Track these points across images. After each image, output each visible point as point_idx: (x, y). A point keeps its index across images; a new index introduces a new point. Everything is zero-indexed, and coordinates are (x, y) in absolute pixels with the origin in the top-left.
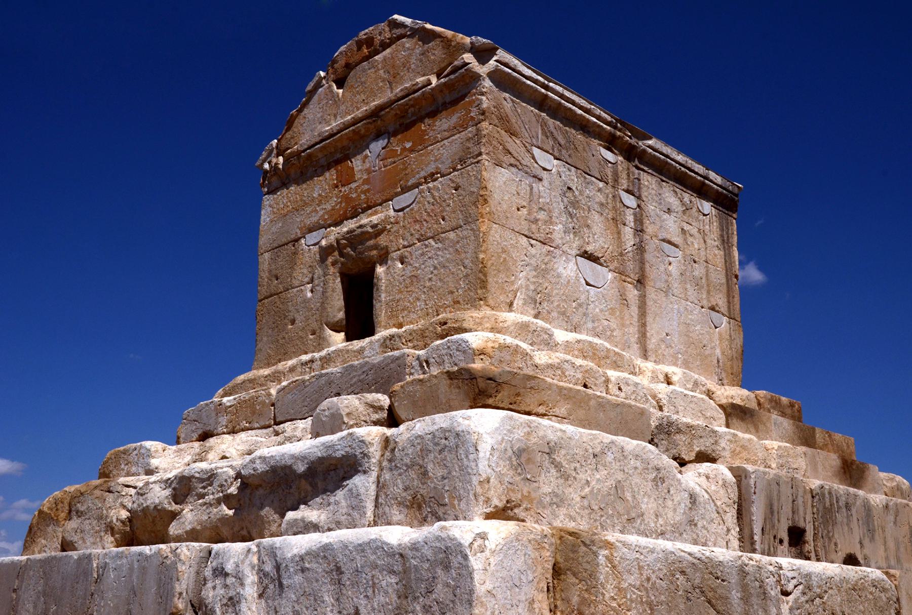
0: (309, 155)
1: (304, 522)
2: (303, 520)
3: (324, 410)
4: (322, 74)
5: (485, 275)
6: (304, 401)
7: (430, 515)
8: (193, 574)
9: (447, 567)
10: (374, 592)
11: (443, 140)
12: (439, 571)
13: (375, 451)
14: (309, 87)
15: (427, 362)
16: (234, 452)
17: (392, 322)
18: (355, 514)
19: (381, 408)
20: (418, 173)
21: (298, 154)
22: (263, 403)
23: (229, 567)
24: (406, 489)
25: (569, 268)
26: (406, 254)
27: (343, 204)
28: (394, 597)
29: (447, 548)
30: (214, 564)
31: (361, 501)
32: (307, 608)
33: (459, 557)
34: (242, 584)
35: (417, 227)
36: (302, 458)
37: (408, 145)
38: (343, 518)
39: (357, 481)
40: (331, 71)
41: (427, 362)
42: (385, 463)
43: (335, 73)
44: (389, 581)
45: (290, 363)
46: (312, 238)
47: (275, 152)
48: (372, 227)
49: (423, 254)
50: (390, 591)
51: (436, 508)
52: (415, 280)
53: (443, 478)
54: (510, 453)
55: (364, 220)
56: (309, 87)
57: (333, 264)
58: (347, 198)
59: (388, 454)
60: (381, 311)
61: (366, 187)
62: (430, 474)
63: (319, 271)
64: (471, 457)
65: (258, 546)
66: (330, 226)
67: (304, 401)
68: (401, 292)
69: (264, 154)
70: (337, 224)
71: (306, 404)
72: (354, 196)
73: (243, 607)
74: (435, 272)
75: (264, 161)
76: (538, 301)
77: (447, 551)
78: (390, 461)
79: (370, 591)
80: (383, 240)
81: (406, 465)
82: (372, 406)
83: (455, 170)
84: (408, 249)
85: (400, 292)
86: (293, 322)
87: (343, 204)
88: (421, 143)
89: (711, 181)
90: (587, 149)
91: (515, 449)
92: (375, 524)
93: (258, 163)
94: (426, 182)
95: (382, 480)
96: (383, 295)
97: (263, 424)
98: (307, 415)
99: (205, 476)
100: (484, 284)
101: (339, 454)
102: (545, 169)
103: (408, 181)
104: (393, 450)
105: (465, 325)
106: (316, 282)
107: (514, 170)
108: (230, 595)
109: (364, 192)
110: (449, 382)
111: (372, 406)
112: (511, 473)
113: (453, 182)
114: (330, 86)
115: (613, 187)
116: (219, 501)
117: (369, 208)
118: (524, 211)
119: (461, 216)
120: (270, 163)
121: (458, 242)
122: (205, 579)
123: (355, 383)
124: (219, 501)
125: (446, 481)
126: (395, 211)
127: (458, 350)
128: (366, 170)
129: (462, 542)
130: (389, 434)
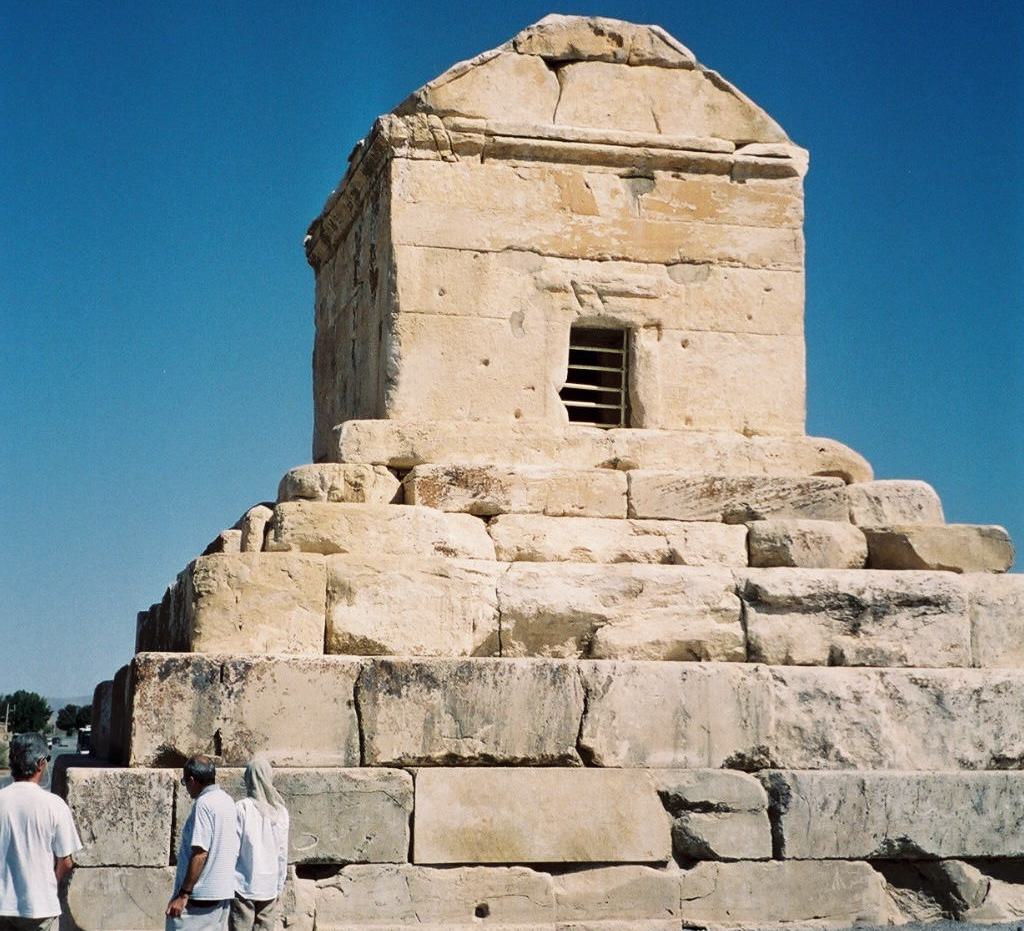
0: (510, 146)
27: (578, 238)
35: (711, 313)
41: (876, 498)
49: (718, 347)
58: (583, 231)
61: (620, 232)
71: (689, 505)
72: (598, 234)
80: (655, 310)
87: (578, 238)
88: (706, 211)
96: (659, 377)
97: (610, 514)
98: (694, 518)
109: (618, 237)
110: (980, 537)
121: (772, 351)
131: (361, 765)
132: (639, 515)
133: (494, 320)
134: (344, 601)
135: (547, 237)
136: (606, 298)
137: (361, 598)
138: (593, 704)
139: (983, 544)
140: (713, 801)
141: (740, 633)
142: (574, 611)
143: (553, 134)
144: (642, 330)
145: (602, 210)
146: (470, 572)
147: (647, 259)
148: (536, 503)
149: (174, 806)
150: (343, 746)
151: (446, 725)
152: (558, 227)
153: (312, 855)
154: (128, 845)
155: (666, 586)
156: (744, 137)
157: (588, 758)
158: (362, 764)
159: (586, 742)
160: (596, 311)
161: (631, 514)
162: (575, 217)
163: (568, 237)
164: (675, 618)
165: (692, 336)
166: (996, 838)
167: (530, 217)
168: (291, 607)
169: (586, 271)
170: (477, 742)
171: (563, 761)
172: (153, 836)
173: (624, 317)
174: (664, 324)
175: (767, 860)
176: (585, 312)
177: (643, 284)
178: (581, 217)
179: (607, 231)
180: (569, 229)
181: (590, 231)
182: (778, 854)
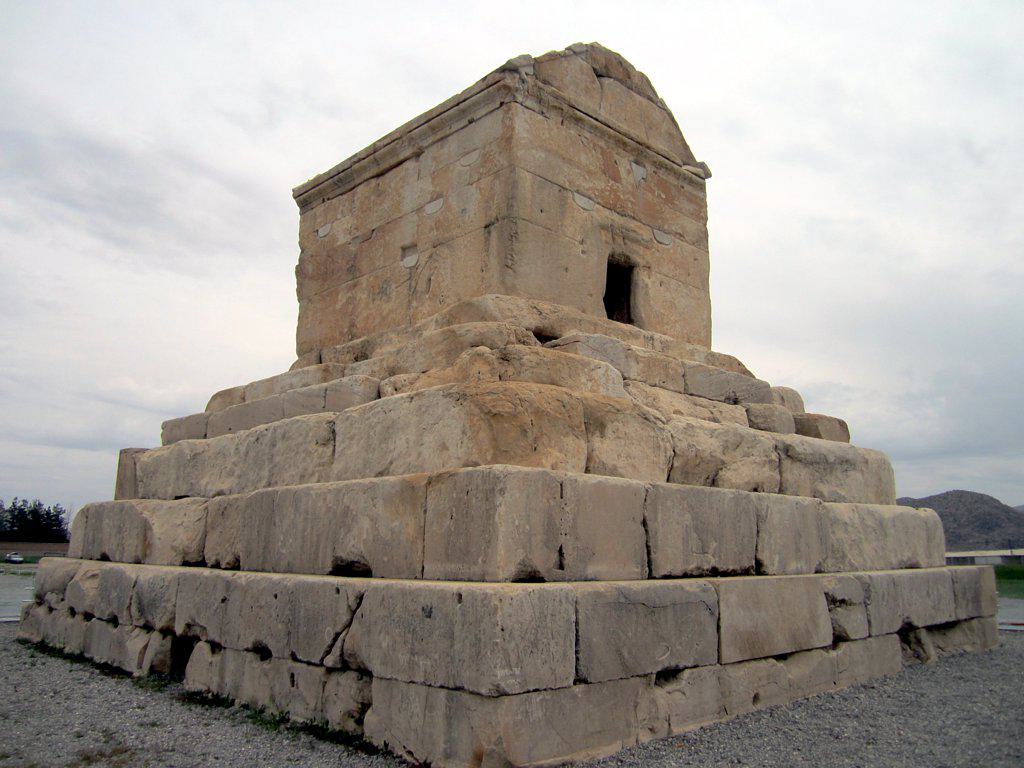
55: (633, 224)
61: (632, 199)
88: (669, 200)
109: (632, 203)
117: (634, 218)
131: (648, 579)
132: (690, 392)
134: (598, 433)
136: (626, 241)
137: (609, 431)
138: (763, 527)
140: (846, 598)
141: (778, 477)
142: (712, 456)
145: (624, 182)
149: (577, 623)
150: (639, 561)
151: (694, 542)
153: (666, 665)
154: (547, 666)
157: (758, 568)
158: (651, 577)
159: (760, 557)
160: (620, 248)
162: (612, 182)
163: (607, 193)
164: (754, 465)
166: (933, 611)
168: (567, 435)
169: (616, 217)
170: (710, 556)
171: (746, 572)
172: (565, 655)
173: (636, 258)
174: (653, 268)
175: (865, 639)
176: (618, 250)
179: (627, 196)
182: (870, 636)
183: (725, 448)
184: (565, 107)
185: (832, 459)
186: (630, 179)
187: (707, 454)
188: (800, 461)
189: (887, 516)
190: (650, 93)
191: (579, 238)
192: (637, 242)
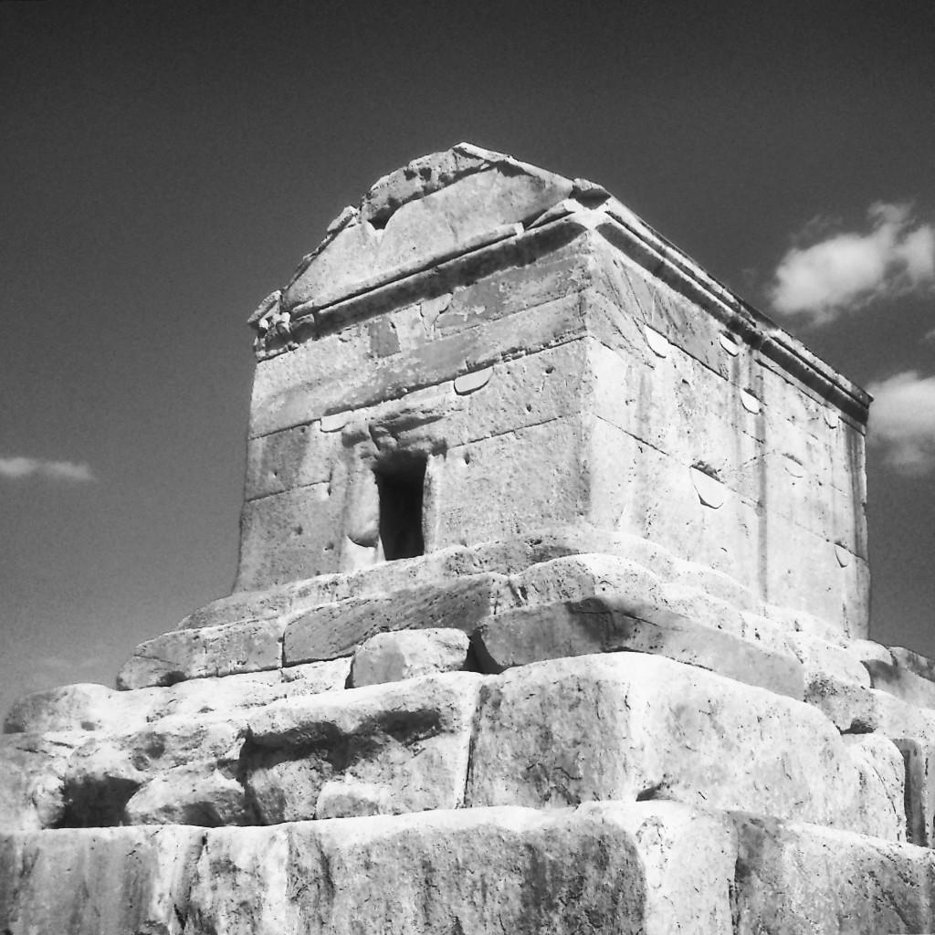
0: (331, 316)
1: (353, 799)
2: (351, 798)
3: (374, 649)
4: (354, 211)
5: (587, 483)
6: (332, 635)
7: (554, 793)
8: (179, 871)
9: (603, 863)
10: (484, 896)
11: (529, 305)
12: (590, 870)
13: (467, 705)
14: (334, 224)
15: (524, 591)
16: (224, 706)
17: (453, 536)
18: (437, 790)
19: (459, 648)
20: (493, 347)
21: (315, 310)
22: (266, 638)
23: (242, 861)
24: (516, 757)
25: (686, 483)
26: (473, 450)
27: (380, 381)
28: (517, 904)
29: (603, 837)
30: (214, 856)
31: (448, 772)
32: (374, 919)
33: (622, 850)
34: (262, 885)
35: (491, 416)
36: (353, 713)
37: (479, 310)
38: (418, 796)
39: (437, 745)
40: (365, 206)
42: (485, 723)
43: (372, 207)
44: (509, 885)
45: (300, 585)
46: (333, 422)
47: (277, 306)
48: (423, 412)
49: (498, 452)
50: (511, 895)
51: (564, 781)
52: (485, 484)
53: (576, 743)
54: (667, 711)
55: (411, 401)
56: (334, 224)
57: (364, 456)
58: (386, 373)
59: (487, 709)
60: (435, 523)
61: (415, 361)
62: (555, 737)
63: (341, 467)
64: (619, 715)
65: (289, 831)
66: (359, 407)
67: (332, 635)
68: (465, 499)
69: (262, 308)
70: (368, 404)
71: (334, 640)
72: (397, 370)
73: (267, 917)
74: (516, 475)
75: (260, 317)
76: (648, 521)
77: (602, 844)
78: (492, 718)
79: (478, 898)
80: (439, 431)
81: (519, 726)
82: (448, 646)
83: (547, 345)
84: (477, 444)
85: (464, 498)
86: (300, 531)
87: (380, 381)
88: (497, 307)
89: (840, 387)
90: (705, 334)
91: (673, 707)
92: (467, 803)
93: (251, 319)
94: (505, 360)
95: (479, 744)
97: (264, 665)
98: (335, 655)
99: (188, 734)
100: (586, 495)
101: (411, 708)
102: (658, 355)
103: (478, 356)
104: (496, 705)
105: (569, 544)
106: (336, 480)
107: (623, 352)
108: (244, 899)
109: (413, 368)
111: (448, 646)
112: (669, 737)
113: (544, 362)
114: (363, 229)
115: (734, 384)
116: (211, 768)
117: (419, 387)
118: (634, 406)
119: (554, 406)
120: (269, 320)
121: (550, 439)
122: (197, 876)
123: (411, 615)
124: (211, 768)
125: (579, 747)
126: (458, 393)
127: (569, 575)
128: (416, 338)
129: (627, 829)
130: (487, 684)
133: (308, 487)
135: (355, 390)
139: (571, 622)
143: (359, 288)
144: (431, 456)
146: (59, 744)
147: (436, 380)
148: (211, 665)
152: (365, 377)
155: (185, 738)
156: (532, 212)
161: (286, 665)
162: (380, 361)
163: (373, 384)
165: (472, 448)
167: (344, 376)
177: (428, 407)
178: (385, 359)
179: (405, 364)
180: (374, 375)
181: (391, 370)
183: (139, 763)
184: (311, 318)
185: (349, 726)
186: (417, 332)
187: (100, 777)
188: (280, 748)
189: (345, 846)
190: (470, 163)
191: (325, 476)
192: (413, 423)
